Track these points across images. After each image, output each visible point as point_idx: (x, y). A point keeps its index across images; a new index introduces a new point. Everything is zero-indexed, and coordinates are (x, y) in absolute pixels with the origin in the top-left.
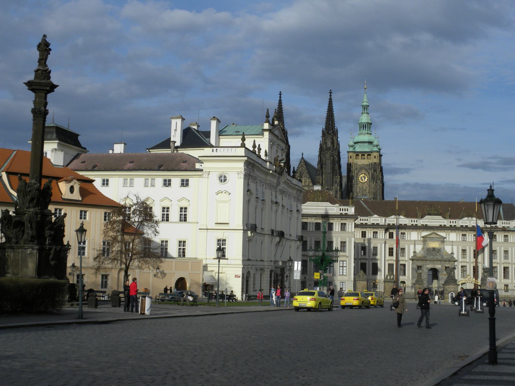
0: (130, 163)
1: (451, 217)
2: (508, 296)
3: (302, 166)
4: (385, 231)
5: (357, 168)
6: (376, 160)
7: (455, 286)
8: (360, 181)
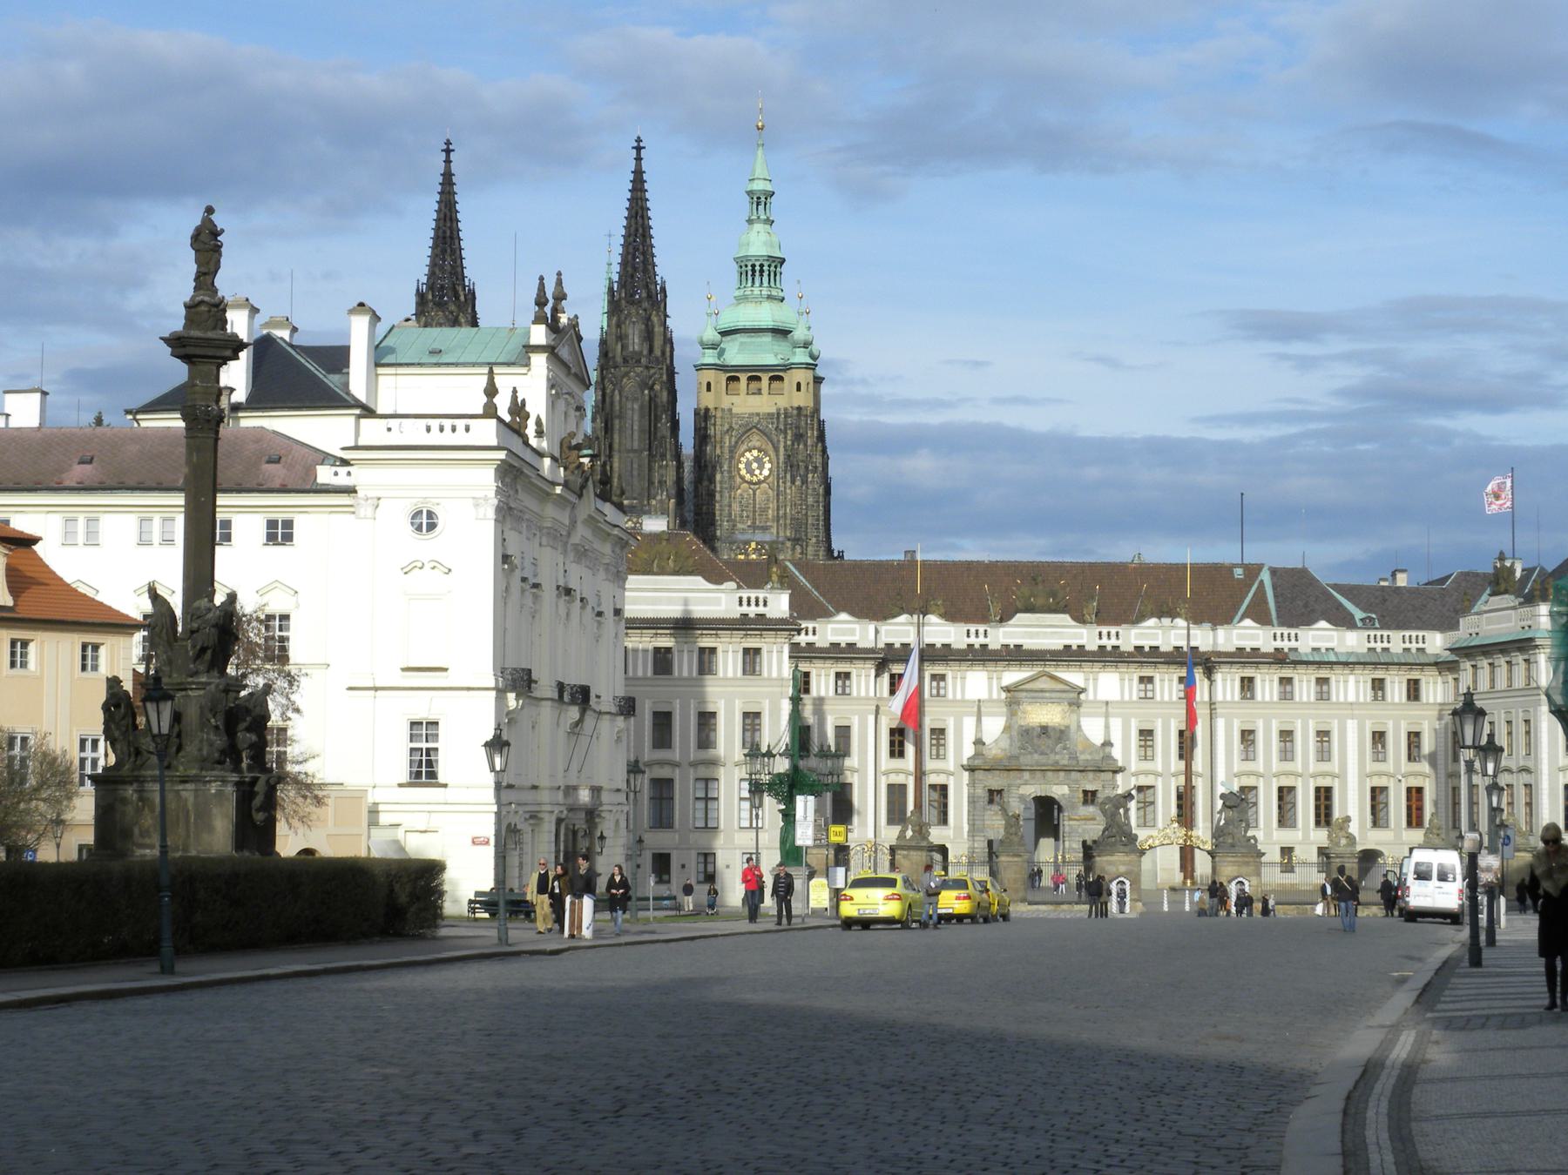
0: (81, 463)
1: (1102, 618)
2: (1292, 885)
4: (876, 670)
5: (731, 428)
6: (803, 400)
7: (1133, 857)
8: (742, 478)
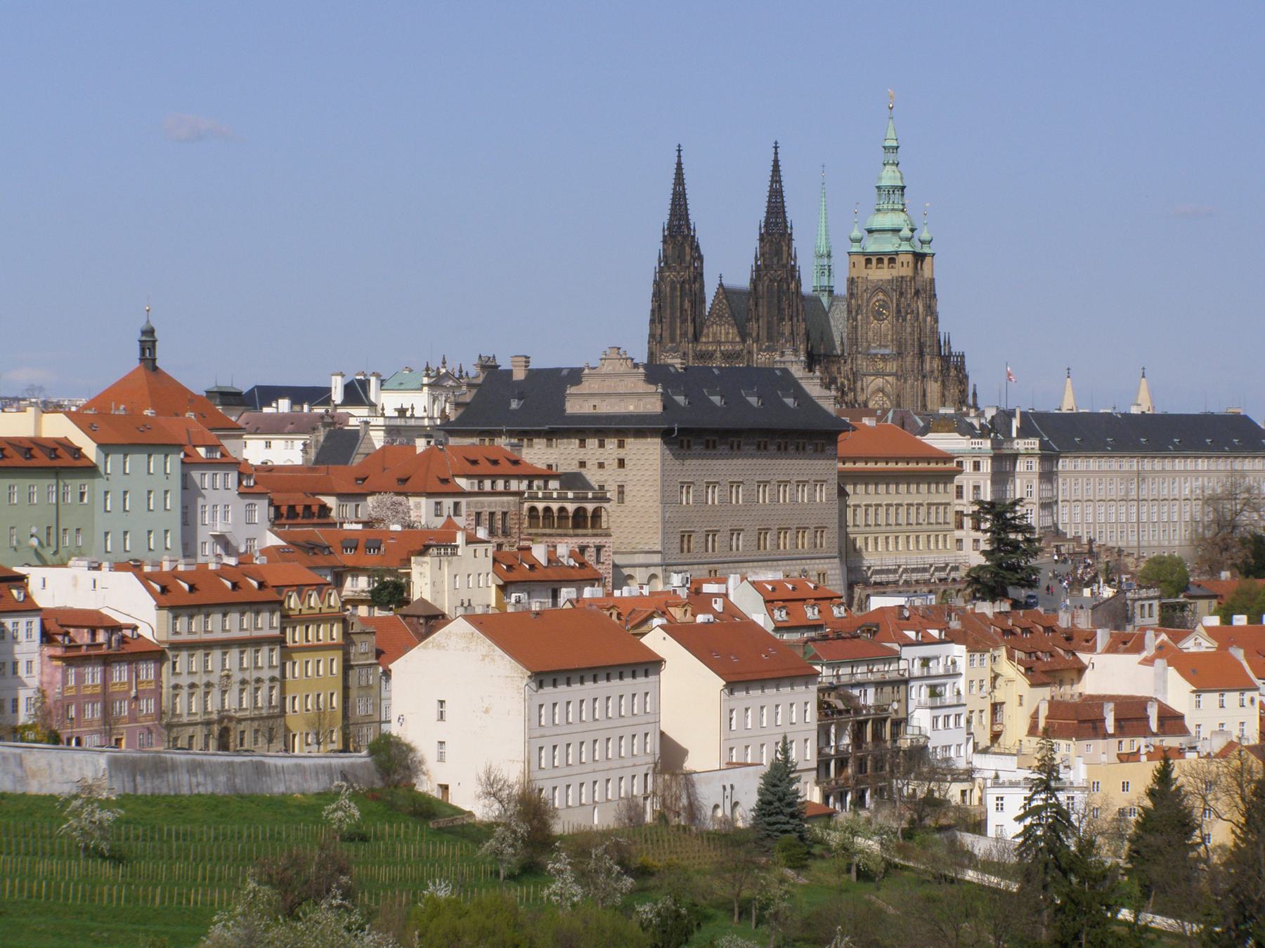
3: (720, 302)
